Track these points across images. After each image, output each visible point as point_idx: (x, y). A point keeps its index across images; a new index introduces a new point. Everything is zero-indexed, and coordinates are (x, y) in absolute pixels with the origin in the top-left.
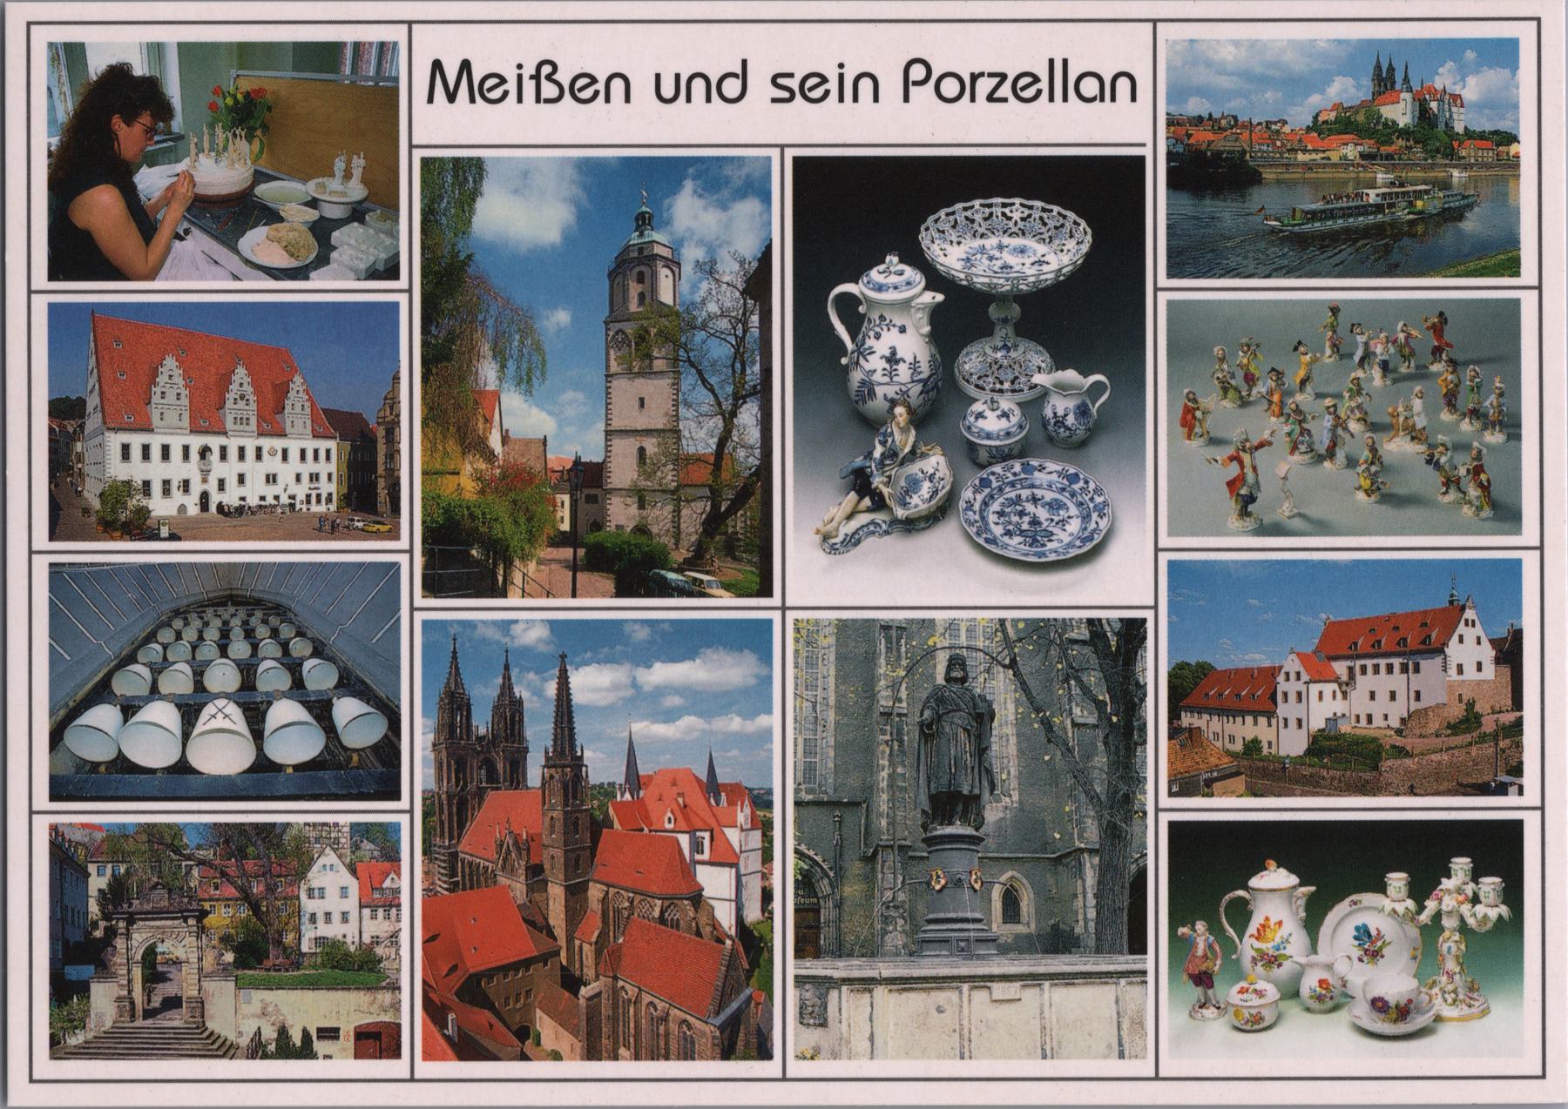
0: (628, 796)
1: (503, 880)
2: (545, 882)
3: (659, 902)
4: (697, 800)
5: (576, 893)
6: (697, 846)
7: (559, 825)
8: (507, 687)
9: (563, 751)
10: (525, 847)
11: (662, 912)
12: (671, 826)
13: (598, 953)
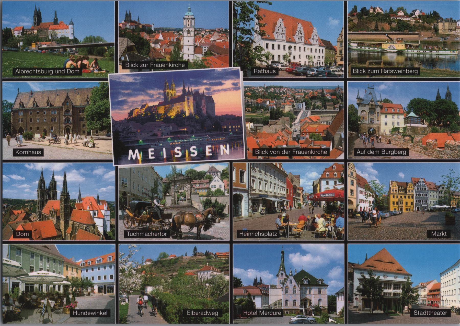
0: (79, 202)
1: (51, 219)
2: (60, 220)
6: (94, 214)
8: (53, 178)
10: (56, 212)
11: (86, 228)
12: (88, 209)
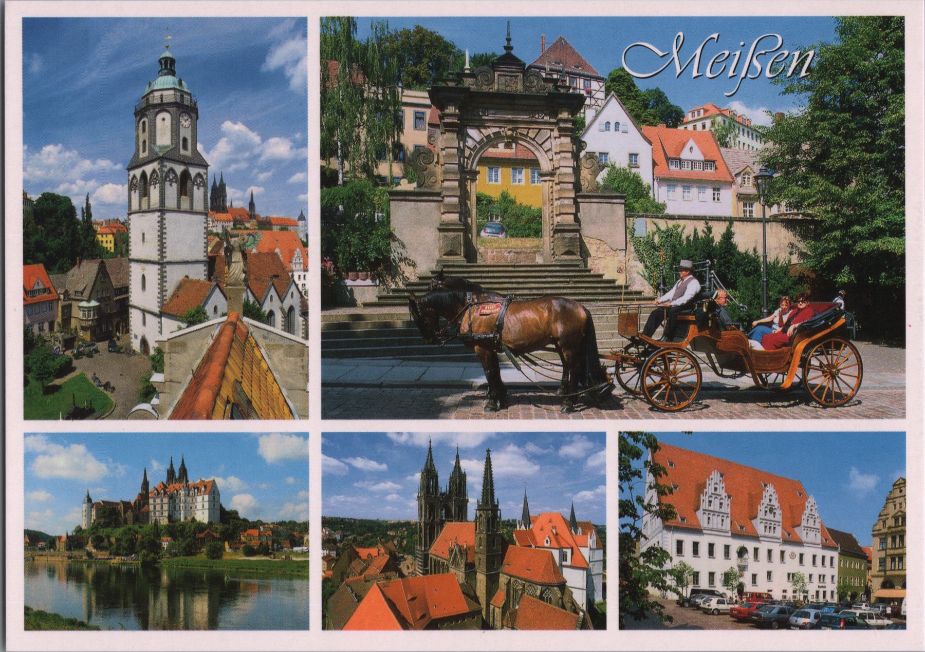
0: (523, 527)
3: (540, 588)
4: (564, 530)
5: (492, 581)
6: (563, 557)
7: (484, 543)
9: (487, 503)
10: (463, 552)
11: (542, 593)
12: (548, 545)
13: (503, 613)
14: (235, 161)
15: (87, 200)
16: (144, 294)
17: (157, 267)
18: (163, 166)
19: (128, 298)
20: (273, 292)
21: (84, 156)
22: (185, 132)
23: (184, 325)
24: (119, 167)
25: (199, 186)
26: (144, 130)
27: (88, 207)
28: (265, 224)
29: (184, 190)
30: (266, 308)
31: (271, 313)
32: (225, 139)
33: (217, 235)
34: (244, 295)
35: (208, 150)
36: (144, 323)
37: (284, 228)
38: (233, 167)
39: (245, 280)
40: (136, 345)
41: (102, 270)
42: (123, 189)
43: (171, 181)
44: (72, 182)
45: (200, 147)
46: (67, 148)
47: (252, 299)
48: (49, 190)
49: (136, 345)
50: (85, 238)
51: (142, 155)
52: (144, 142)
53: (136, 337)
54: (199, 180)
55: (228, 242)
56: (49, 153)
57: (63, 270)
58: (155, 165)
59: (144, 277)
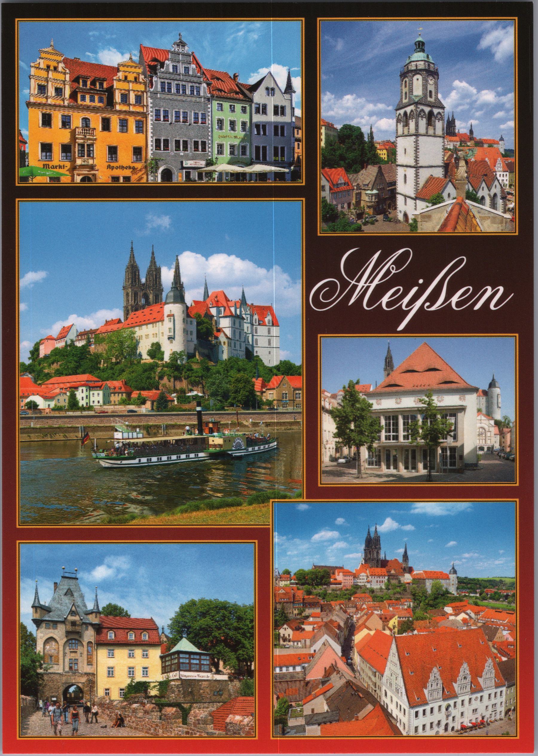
14: (460, 105)
15: (371, 128)
16: (405, 186)
17: (414, 169)
18: (417, 107)
19: (395, 189)
20: (484, 185)
21: (369, 101)
22: (431, 87)
23: (430, 205)
24: (390, 108)
25: (439, 120)
26: (406, 87)
27: (371, 133)
28: (479, 143)
29: (430, 123)
30: (480, 194)
31: (483, 198)
32: (455, 91)
33: (450, 150)
34: (467, 187)
35: (444, 97)
36: (406, 204)
37: (490, 146)
38: (460, 108)
39: (467, 178)
40: (401, 217)
41: (380, 173)
42: (392, 122)
43: (422, 117)
44: (362, 118)
45: (440, 96)
46: (359, 96)
47: (471, 189)
48: (348, 123)
49: (401, 217)
50: (370, 152)
51: (404, 101)
52: (406, 93)
53: (401, 212)
54: (439, 116)
55: (457, 155)
56: (348, 100)
57: (356, 172)
58: (412, 107)
59: (405, 175)
